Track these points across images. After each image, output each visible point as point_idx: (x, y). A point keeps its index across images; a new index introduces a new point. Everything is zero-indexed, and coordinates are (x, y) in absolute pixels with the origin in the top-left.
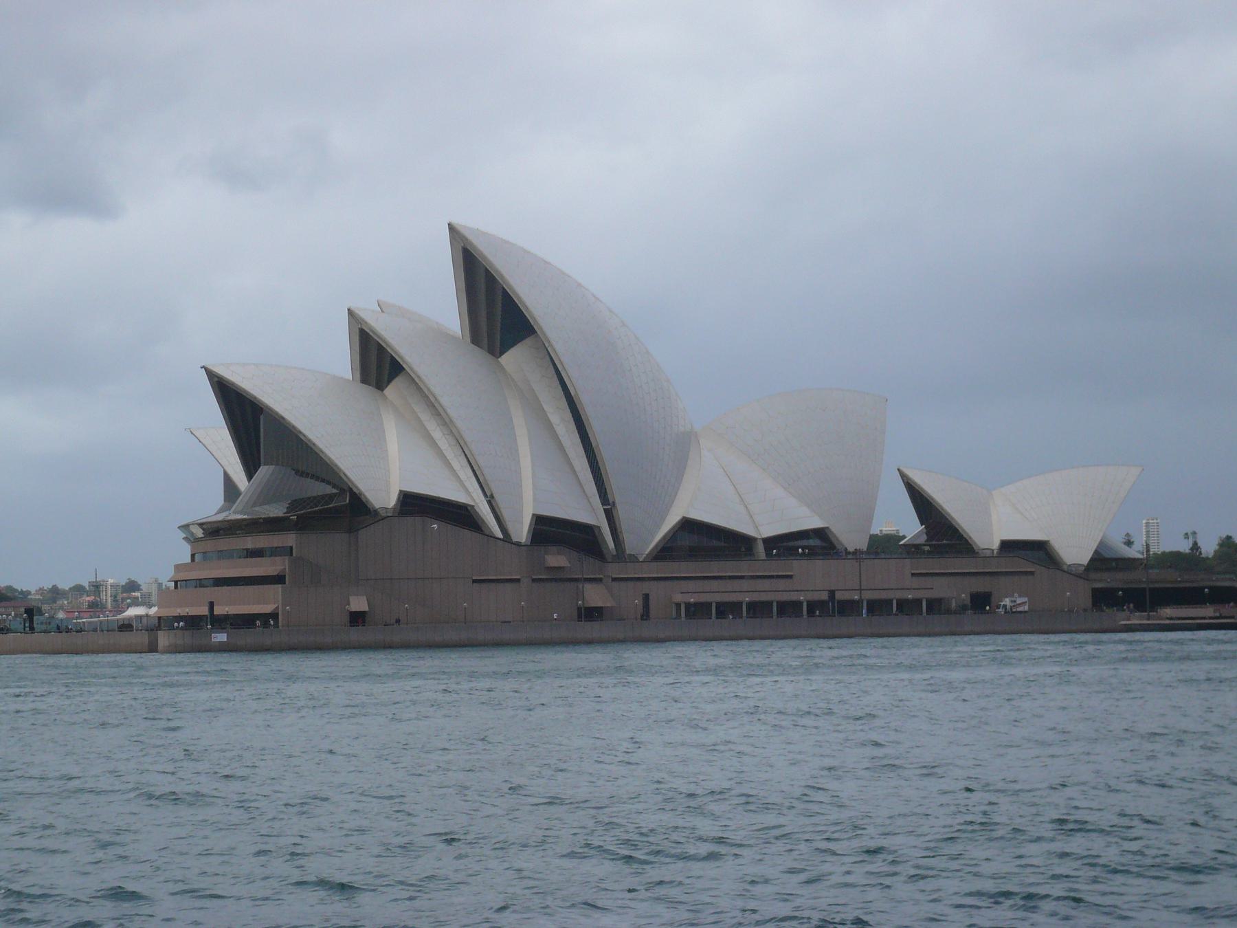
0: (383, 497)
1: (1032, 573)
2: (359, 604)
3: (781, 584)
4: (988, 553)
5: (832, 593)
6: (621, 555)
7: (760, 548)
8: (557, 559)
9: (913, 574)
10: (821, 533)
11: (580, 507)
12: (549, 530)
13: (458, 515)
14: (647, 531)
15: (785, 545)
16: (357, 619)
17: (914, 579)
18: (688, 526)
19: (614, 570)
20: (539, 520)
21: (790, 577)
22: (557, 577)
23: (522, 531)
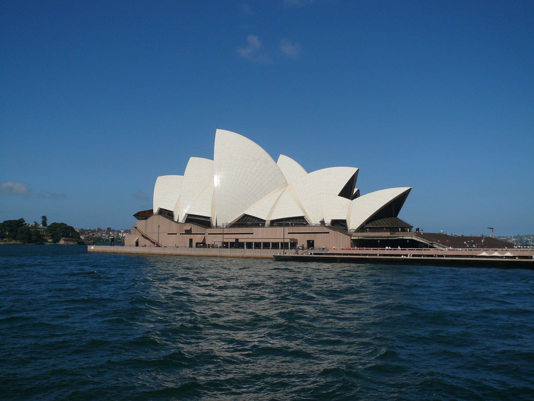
1: (328, 233)
4: (326, 225)
5: (237, 240)
6: (217, 226)
7: (268, 223)
8: (188, 227)
9: (289, 233)
10: (302, 218)
19: (209, 231)
20: (189, 215)
21: (252, 234)
22: (188, 232)
23: (181, 219)
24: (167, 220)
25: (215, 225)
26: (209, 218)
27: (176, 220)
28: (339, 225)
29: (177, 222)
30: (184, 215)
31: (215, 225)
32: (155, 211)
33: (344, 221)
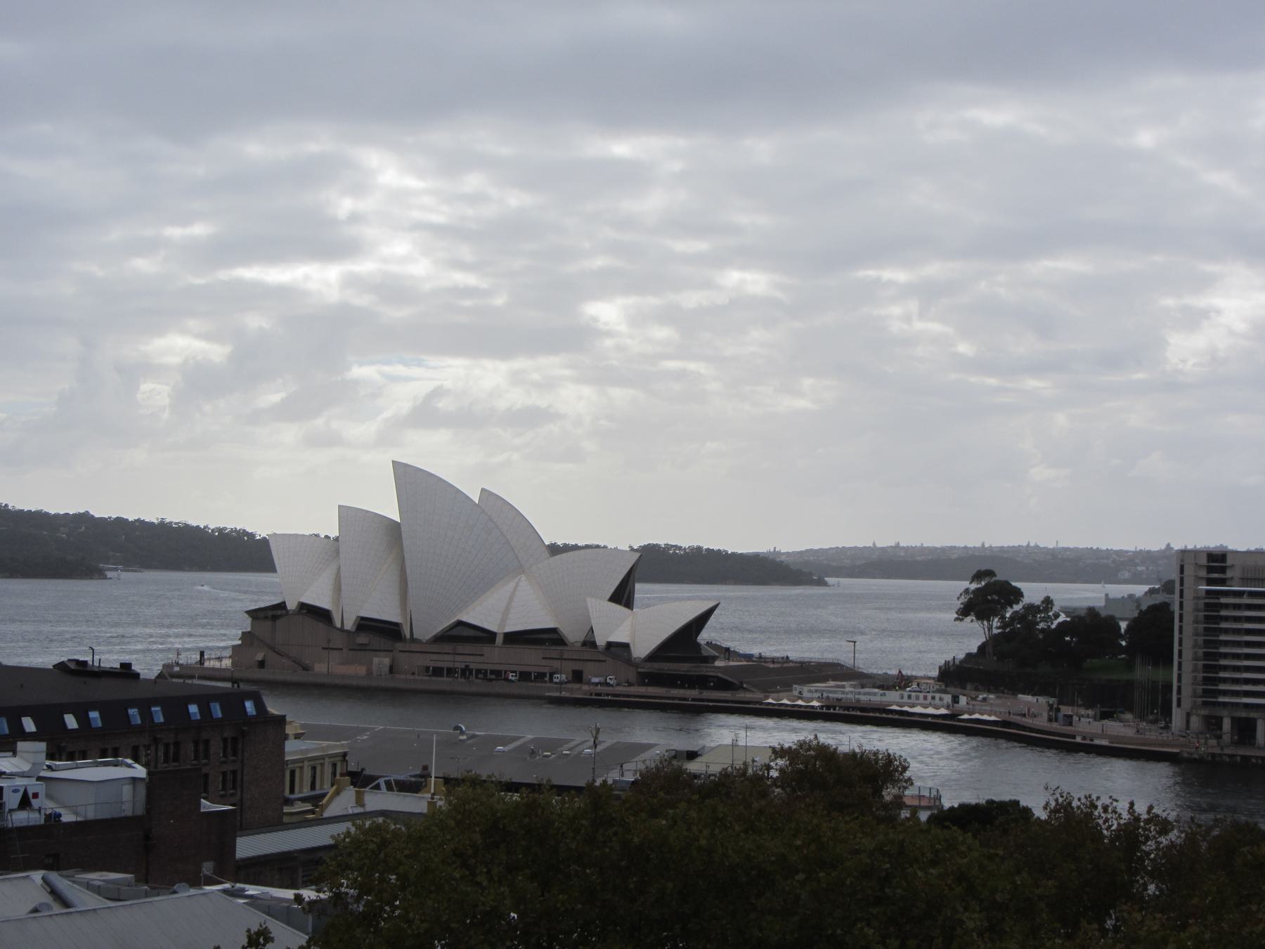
0: (291, 606)
2: (260, 657)
3: (478, 659)
7: (499, 640)
8: (362, 639)
10: (554, 630)
11: (390, 613)
12: (366, 625)
13: (322, 615)
14: (427, 626)
15: (514, 638)
16: (262, 664)
17: (544, 662)
18: (460, 623)
19: (399, 646)
20: (363, 619)
23: (349, 625)
24: (321, 625)
25: (408, 636)
26: (397, 624)
27: (338, 625)
28: (619, 650)
29: (342, 630)
30: (354, 618)
31: (408, 636)
32: (291, 606)
33: (626, 646)
